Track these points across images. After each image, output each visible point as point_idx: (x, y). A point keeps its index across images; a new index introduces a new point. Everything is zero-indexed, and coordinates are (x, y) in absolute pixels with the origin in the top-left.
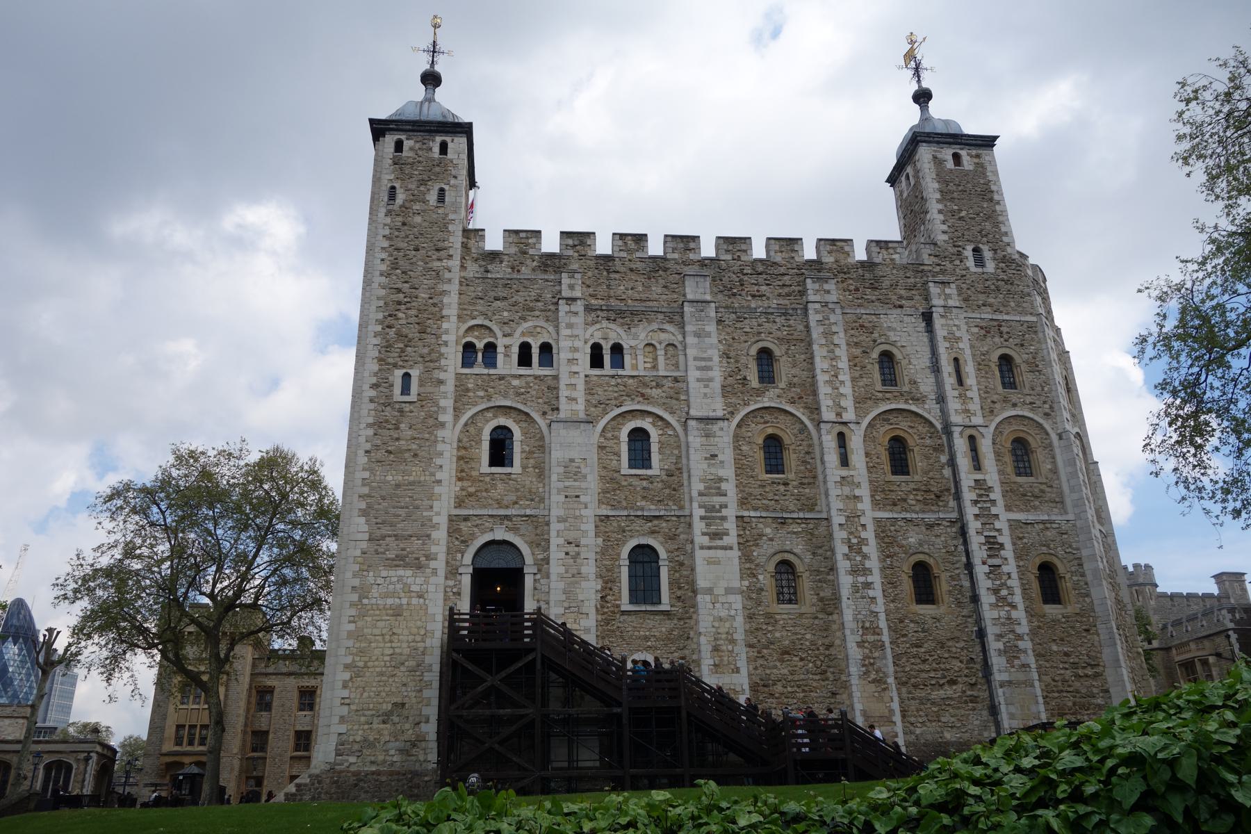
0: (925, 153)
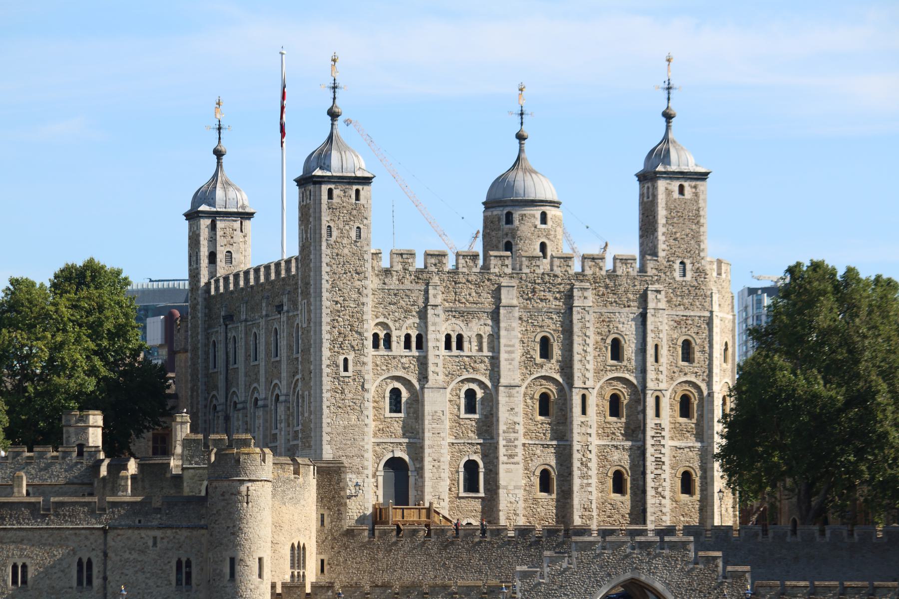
0: (662, 184)
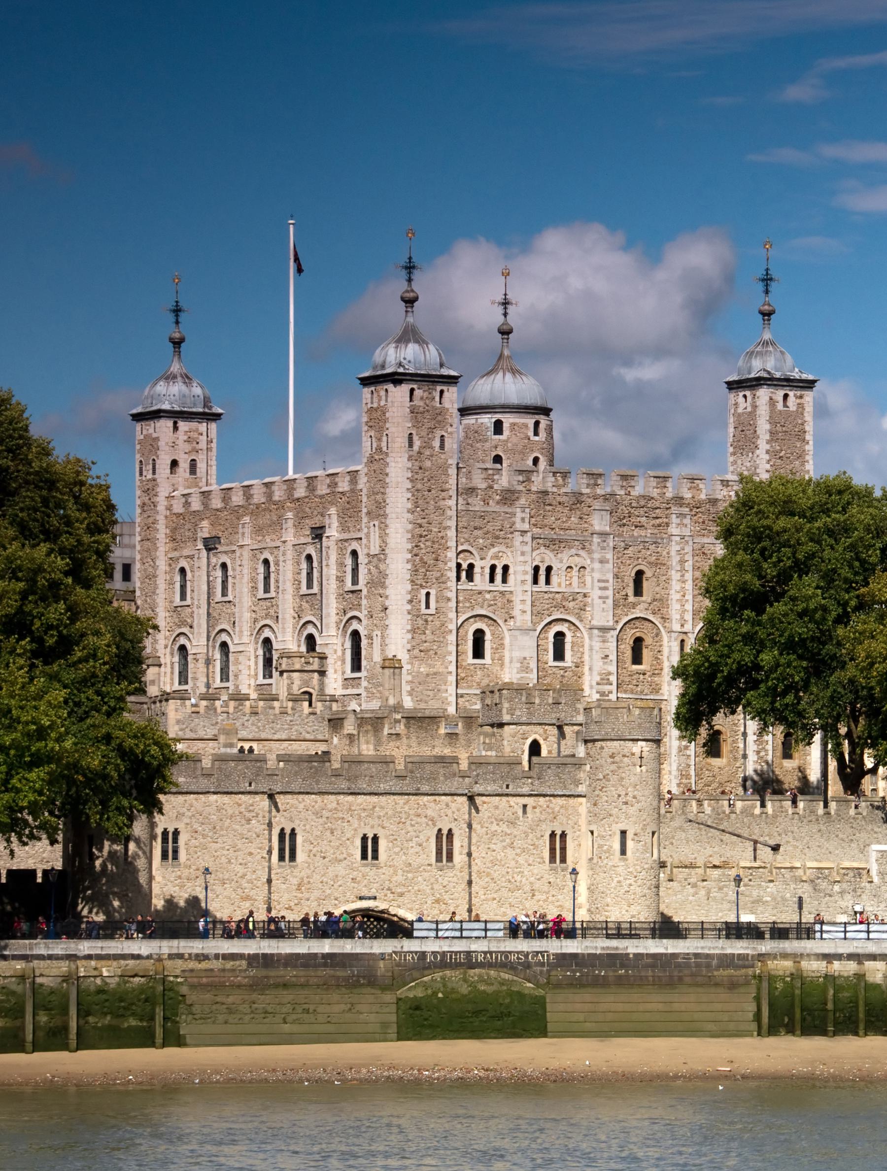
0: (764, 393)
